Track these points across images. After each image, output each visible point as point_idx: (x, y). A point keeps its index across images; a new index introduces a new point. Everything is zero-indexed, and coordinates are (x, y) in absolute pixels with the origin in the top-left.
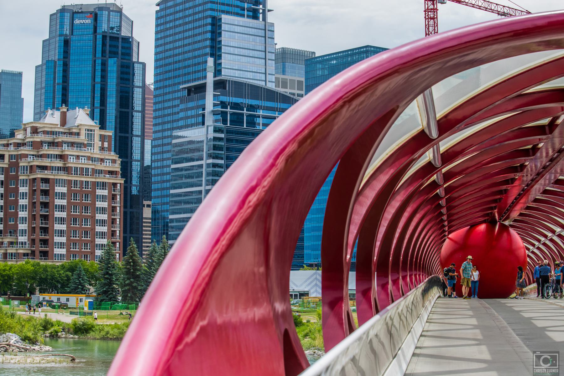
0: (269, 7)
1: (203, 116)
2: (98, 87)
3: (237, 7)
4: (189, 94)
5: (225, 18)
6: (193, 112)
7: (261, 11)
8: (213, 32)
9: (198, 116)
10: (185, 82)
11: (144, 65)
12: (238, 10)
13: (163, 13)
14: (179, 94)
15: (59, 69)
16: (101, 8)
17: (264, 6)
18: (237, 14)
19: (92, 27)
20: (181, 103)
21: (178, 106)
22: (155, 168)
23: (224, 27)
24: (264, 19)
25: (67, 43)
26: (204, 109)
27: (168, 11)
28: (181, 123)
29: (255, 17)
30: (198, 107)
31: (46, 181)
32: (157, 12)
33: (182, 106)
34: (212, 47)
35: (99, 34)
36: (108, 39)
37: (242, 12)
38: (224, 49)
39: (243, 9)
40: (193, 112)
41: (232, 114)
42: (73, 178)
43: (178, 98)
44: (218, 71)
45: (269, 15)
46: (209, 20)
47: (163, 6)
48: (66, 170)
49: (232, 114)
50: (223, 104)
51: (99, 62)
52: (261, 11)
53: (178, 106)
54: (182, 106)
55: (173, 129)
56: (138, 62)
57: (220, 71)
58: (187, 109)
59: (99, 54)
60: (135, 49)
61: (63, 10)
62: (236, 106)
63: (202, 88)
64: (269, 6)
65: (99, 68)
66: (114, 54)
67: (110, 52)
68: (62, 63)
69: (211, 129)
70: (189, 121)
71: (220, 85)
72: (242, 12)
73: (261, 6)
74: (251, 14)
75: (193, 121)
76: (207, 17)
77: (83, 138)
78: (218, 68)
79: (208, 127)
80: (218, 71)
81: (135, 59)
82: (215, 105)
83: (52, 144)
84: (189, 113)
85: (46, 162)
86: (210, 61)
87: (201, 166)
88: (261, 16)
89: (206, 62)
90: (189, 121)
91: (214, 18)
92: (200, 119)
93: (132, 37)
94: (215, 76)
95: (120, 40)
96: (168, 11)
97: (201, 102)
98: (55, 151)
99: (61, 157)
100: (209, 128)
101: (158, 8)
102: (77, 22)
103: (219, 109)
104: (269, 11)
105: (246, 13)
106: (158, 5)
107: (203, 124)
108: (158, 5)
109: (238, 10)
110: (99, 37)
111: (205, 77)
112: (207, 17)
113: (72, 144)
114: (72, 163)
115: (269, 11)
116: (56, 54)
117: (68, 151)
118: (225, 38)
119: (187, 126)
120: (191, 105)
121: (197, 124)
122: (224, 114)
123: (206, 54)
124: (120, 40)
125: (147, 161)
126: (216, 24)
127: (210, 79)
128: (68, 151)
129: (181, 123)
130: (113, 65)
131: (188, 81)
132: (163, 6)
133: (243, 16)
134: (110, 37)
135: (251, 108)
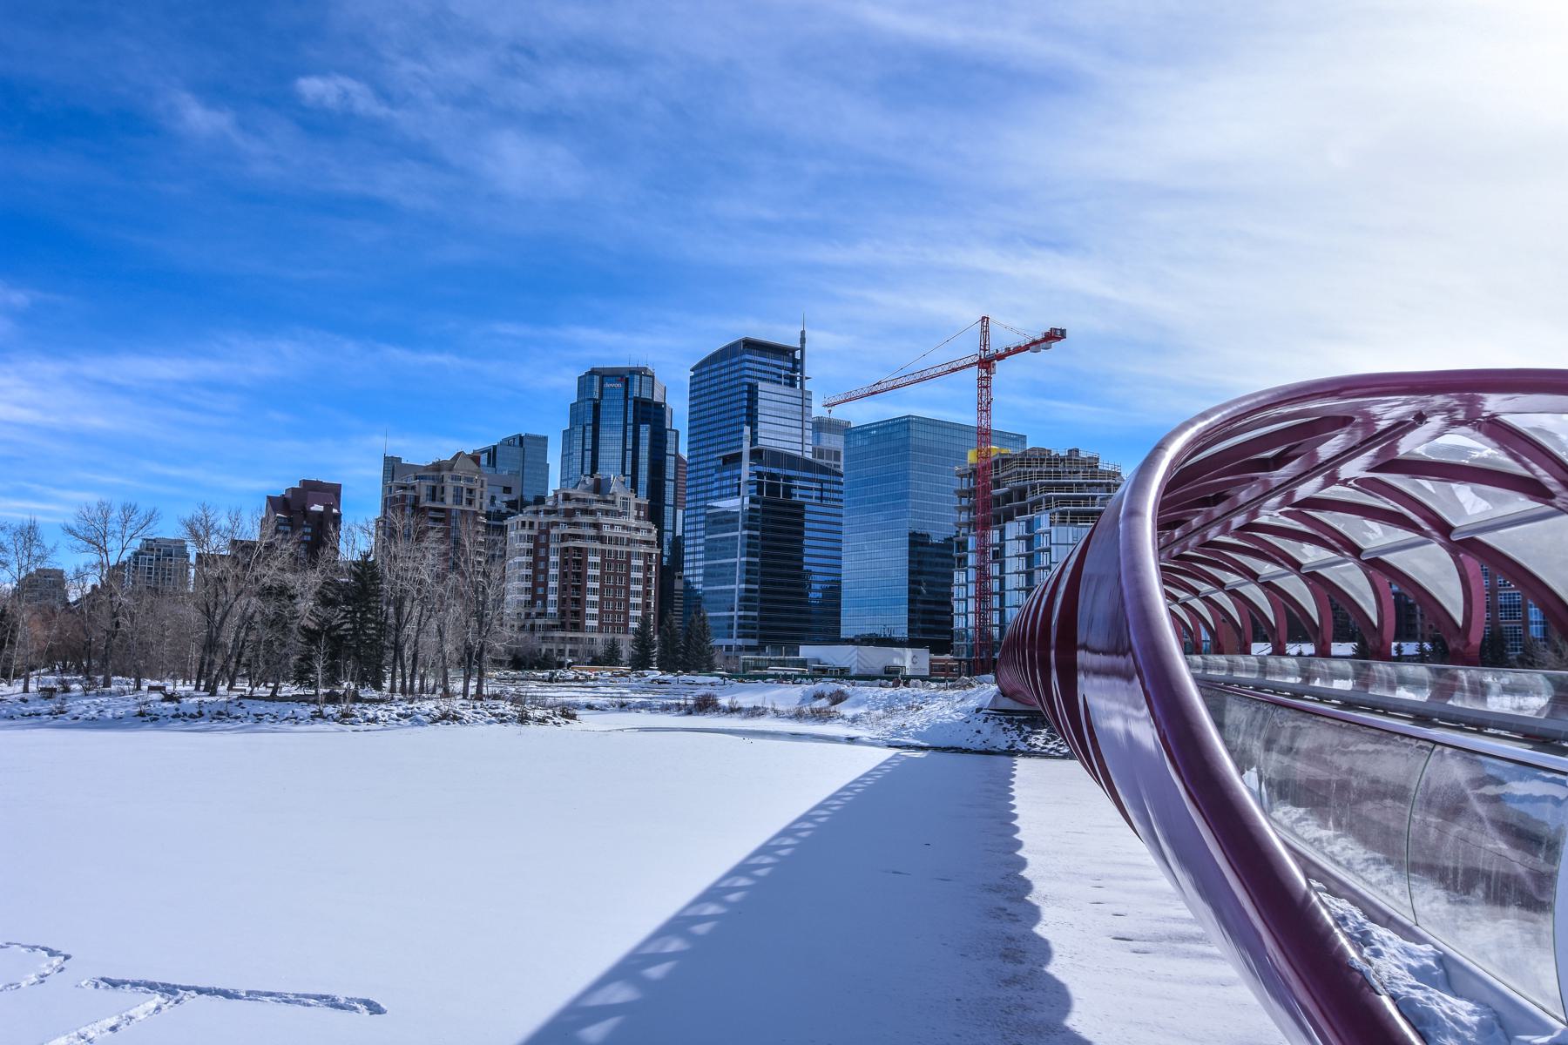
0: (806, 375)
1: (739, 485)
2: (629, 454)
3: (774, 373)
4: (724, 464)
5: (761, 385)
6: (728, 482)
7: (798, 379)
8: (748, 400)
9: (733, 486)
10: (719, 451)
11: (677, 432)
12: (775, 377)
13: (697, 379)
14: (713, 464)
16: (633, 372)
17: (802, 373)
18: (774, 381)
19: (623, 392)
20: (716, 472)
21: (713, 475)
22: (688, 539)
23: (760, 394)
24: (802, 387)
25: (597, 408)
26: (739, 479)
27: (703, 377)
28: (715, 493)
29: (793, 385)
30: (733, 477)
32: (691, 378)
33: (717, 476)
34: (748, 415)
35: (631, 399)
36: (640, 404)
37: (779, 380)
38: (760, 418)
39: (780, 376)
40: (728, 482)
41: (768, 484)
43: (713, 467)
44: (754, 440)
45: (806, 381)
46: (746, 388)
47: (697, 372)
49: (768, 484)
50: (759, 474)
51: (630, 428)
52: (798, 379)
53: (713, 475)
54: (717, 476)
55: (706, 499)
56: (671, 430)
57: (756, 440)
58: (722, 479)
59: (630, 421)
60: (668, 415)
61: (593, 372)
62: (772, 476)
63: (736, 459)
65: (630, 434)
67: (642, 419)
68: (591, 428)
69: (747, 500)
70: (724, 492)
71: (757, 455)
72: (779, 380)
73: (799, 374)
74: (788, 381)
75: (728, 491)
76: (743, 384)
78: (754, 437)
79: (743, 497)
80: (754, 440)
81: (667, 427)
82: (751, 475)
84: (725, 483)
86: (747, 430)
88: (798, 383)
89: (742, 430)
90: (724, 492)
91: (750, 385)
92: (736, 489)
93: (665, 404)
94: (751, 446)
95: (653, 406)
96: (703, 377)
97: (736, 472)
100: (745, 498)
101: (692, 373)
102: (607, 385)
103: (755, 478)
104: (807, 378)
105: (783, 380)
106: (692, 370)
107: (739, 494)
108: (692, 370)
109: (775, 377)
110: (631, 402)
111: (741, 446)
112: (743, 384)
115: (807, 378)
119: (720, 497)
120: (727, 474)
121: (731, 495)
122: (760, 484)
123: (742, 423)
124: (653, 406)
125: (679, 533)
126: (753, 391)
127: (746, 447)
129: (715, 493)
130: (645, 431)
131: (723, 450)
132: (697, 372)
133: (780, 383)
134: (642, 402)
135: (788, 478)
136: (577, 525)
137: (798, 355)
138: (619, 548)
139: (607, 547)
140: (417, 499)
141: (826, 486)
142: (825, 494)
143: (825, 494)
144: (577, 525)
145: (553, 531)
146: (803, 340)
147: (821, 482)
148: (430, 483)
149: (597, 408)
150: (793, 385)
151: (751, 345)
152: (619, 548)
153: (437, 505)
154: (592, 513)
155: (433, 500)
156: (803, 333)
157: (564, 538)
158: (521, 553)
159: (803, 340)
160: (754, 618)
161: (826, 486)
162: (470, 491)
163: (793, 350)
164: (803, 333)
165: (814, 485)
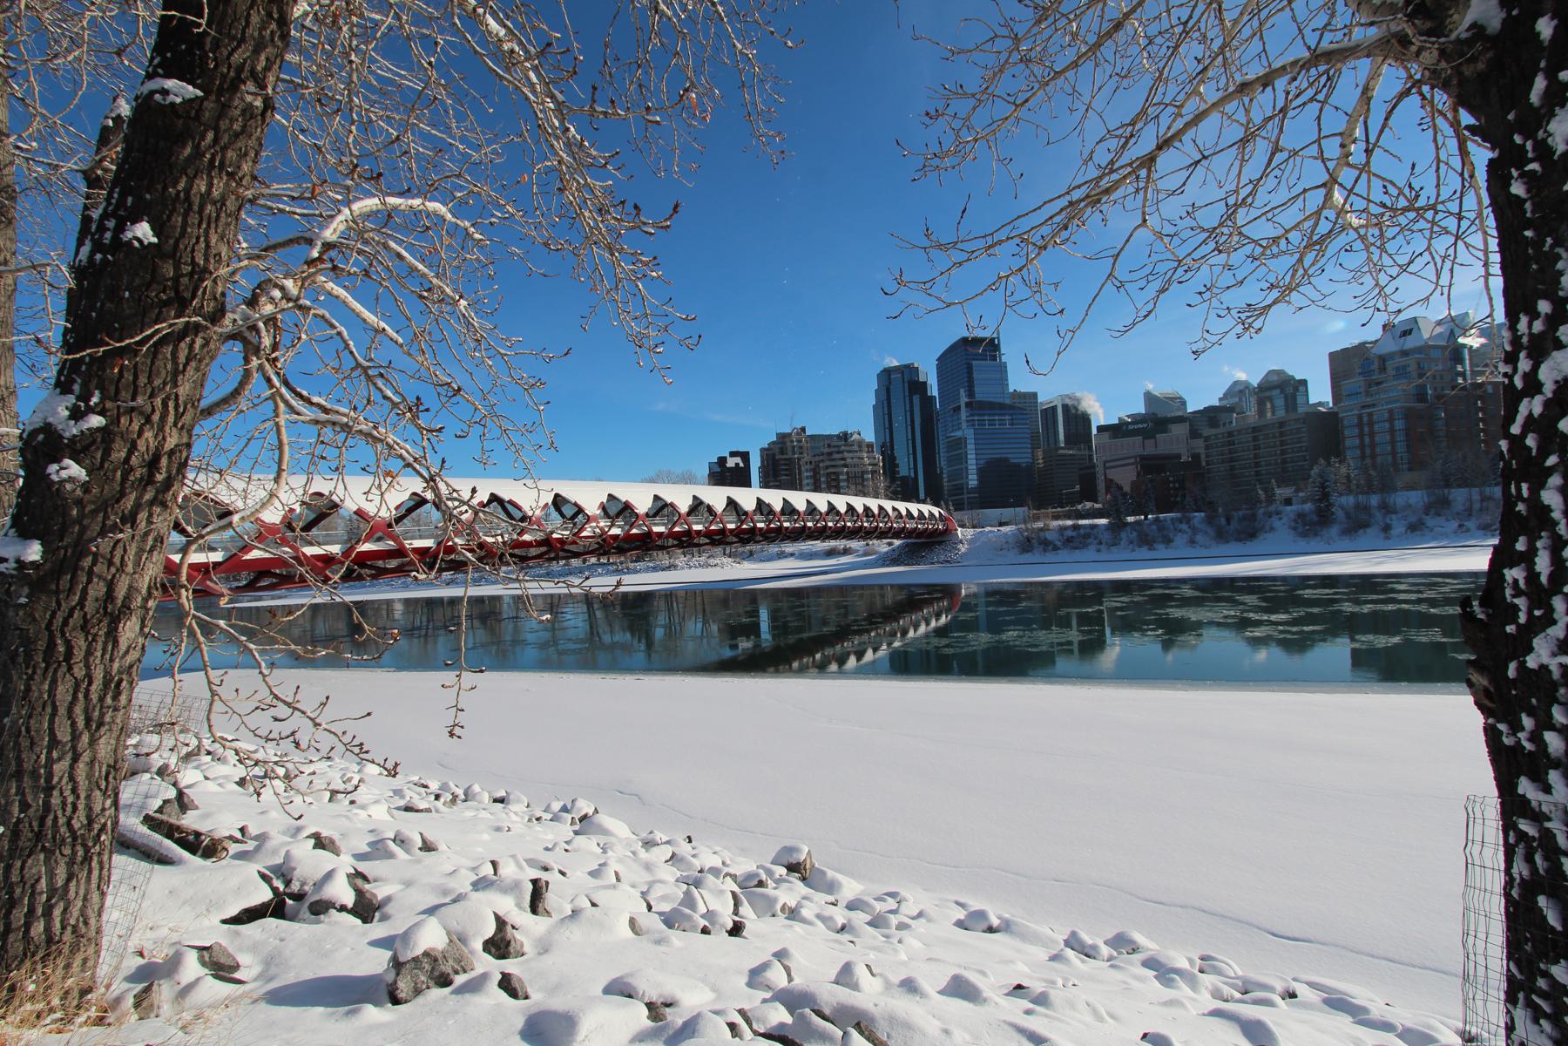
17: (999, 350)
25: (888, 390)
42: (850, 470)
48: (846, 466)
64: (1003, 351)
77: (856, 448)
80: (971, 394)
83: (838, 453)
98: (840, 456)
99: (844, 459)
113: (850, 452)
114: (849, 461)
117: (846, 455)
118: (975, 375)
127: (964, 399)
128: (846, 455)
130: (916, 399)
139: (850, 470)
140: (774, 455)
149: (888, 390)
151: (965, 340)
157: (827, 467)
162: (801, 447)
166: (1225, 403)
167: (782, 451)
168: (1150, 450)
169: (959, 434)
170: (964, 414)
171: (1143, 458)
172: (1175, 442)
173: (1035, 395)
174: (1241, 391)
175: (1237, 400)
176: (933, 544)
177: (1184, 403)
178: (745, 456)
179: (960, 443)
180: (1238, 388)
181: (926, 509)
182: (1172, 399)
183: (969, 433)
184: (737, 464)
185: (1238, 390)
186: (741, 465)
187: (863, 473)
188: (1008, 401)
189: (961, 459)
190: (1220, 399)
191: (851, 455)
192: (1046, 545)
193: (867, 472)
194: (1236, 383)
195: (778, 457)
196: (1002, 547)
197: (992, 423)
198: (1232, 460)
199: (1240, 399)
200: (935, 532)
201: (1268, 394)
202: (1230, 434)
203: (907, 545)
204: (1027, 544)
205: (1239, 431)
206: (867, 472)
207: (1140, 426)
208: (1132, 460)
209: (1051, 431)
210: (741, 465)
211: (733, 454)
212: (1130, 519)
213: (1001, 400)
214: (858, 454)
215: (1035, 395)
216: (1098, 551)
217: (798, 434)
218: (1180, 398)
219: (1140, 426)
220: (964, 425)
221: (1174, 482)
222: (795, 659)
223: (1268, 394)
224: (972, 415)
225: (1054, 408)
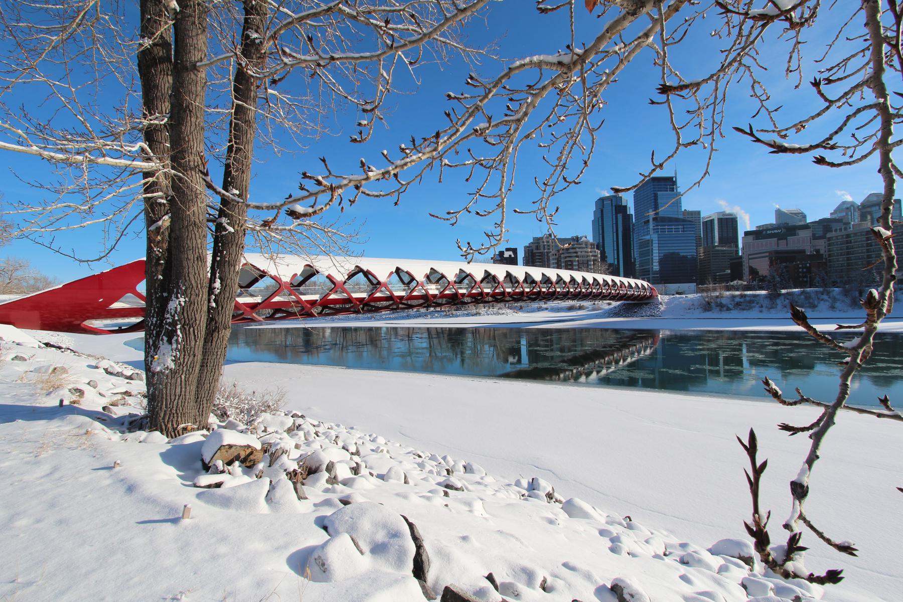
5: (659, 193)
15: (600, 221)
17: (676, 185)
24: (676, 190)
25: (602, 211)
31: (570, 261)
34: (655, 205)
42: (580, 259)
45: (678, 189)
46: (653, 195)
48: (577, 257)
51: (614, 216)
59: (614, 213)
66: (620, 213)
77: (584, 246)
81: (628, 213)
85: (570, 255)
87: (649, 250)
91: (655, 194)
102: (605, 203)
110: (614, 208)
113: (579, 248)
114: (579, 254)
116: (599, 215)
117: (578, 250)
119: (644, 235)
120: (645, 227)
128: (578, 250)
130: (620, 216)
136: (570, 253)
137: (674, 180)
138: (584, 259)
139: (580, 259)
140: (532, 250)
141: (685, 226)
142: (685, 229)
143: (685, 229)
144: (570, 253)
145: (562, 256)
146: (676, 174)
147: (683, 225)
148: (536, 245)
149: (602, 211)
150: (672, 190)
152: (584, 259)
153: (539, 251)
154: (575, 248)
155: (538, 249)
156: (676, 170)
157: (566, 257)
158: (553, 263)
159: (676, 174)
160: (657, 277)
161: (685, 226)
162: (549, 246)
163: (672, 178)
164: (676, 170)
165: (680, 227)
166: (834, 216)
167: (538, 248)
168: (782, 246)
169: (648, 237)
170: (651, 225)
171: (777, 252)
172: (801, 242)
173: (699, 213)
174: (848, 208)
175: (844, 214)
176: (642, 304)
177: (804, 217)
178: (515, 251)
179: (648, 243)
180: (845, 206)
181: (640, 282)
182: (795, 214)
183: (655, 237)
184: (510, 256)
185: (846, 207)
186: (513, 256)
187: (588, 261)
188: (681, 217)
189: (649, 253)
190: (831, 214)
191: (581, 250)
192: (721, 307)
193: (590, 261)
194: (844, 203)
195: (535, 251)
196: (691, 307)
197: (670, 230)
198: (848, 253)
199: (847, 214)
200: (644, 297)
201: (869, 210)
202: (848, 236)
203: (624, 305)
204: (707, 307)
205: (855, 234)
206: (590, 261)
207: (776, 231)
208: (767, 254)
209: (710, 235)
210: (513, 256)
211: (508, 250)
212: (783, 291)
213: (676, 216)
214: (585, 250)
215: (699, 213)
216: (761, 311)
217: (547, 238)
218: (802, 213)
219: (776, 231)
220: (651, 232)
221: (803, 268)
222: (562, 373)
223: (869, 210)
224: (657, 226)
225: (712, 221)
